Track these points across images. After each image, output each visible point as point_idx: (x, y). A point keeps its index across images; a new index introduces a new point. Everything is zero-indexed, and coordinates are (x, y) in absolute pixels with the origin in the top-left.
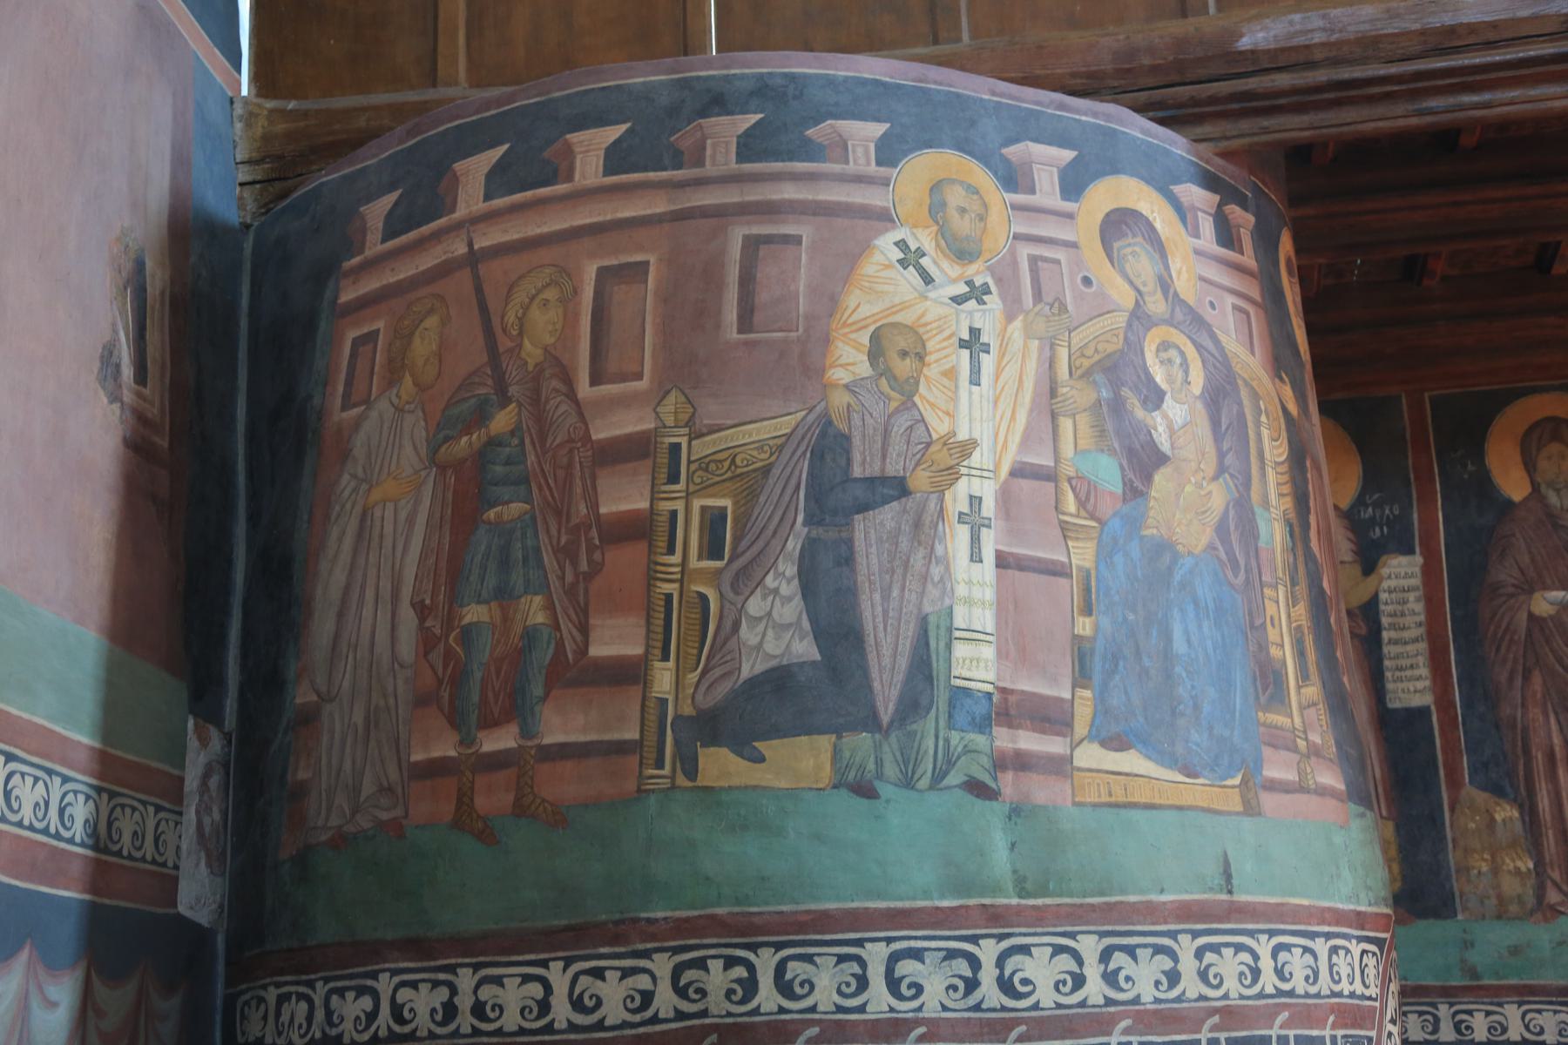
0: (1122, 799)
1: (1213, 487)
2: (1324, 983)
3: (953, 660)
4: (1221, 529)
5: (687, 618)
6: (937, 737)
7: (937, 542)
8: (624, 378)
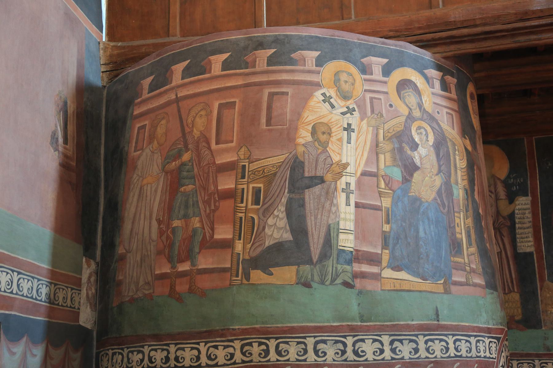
0: (399, 288)
1: (437, 177)
2: (474, 353)
3: (339, 240)
4: (439, 193)
5: (247, 225)
6: (333, 267)
7: (334, 199)
8: (227, 142)
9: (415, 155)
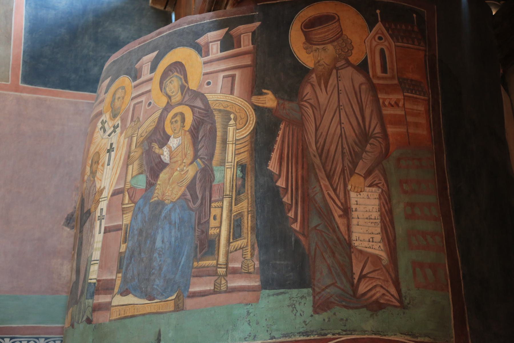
1: (190, 167)
9: (163, 151)
